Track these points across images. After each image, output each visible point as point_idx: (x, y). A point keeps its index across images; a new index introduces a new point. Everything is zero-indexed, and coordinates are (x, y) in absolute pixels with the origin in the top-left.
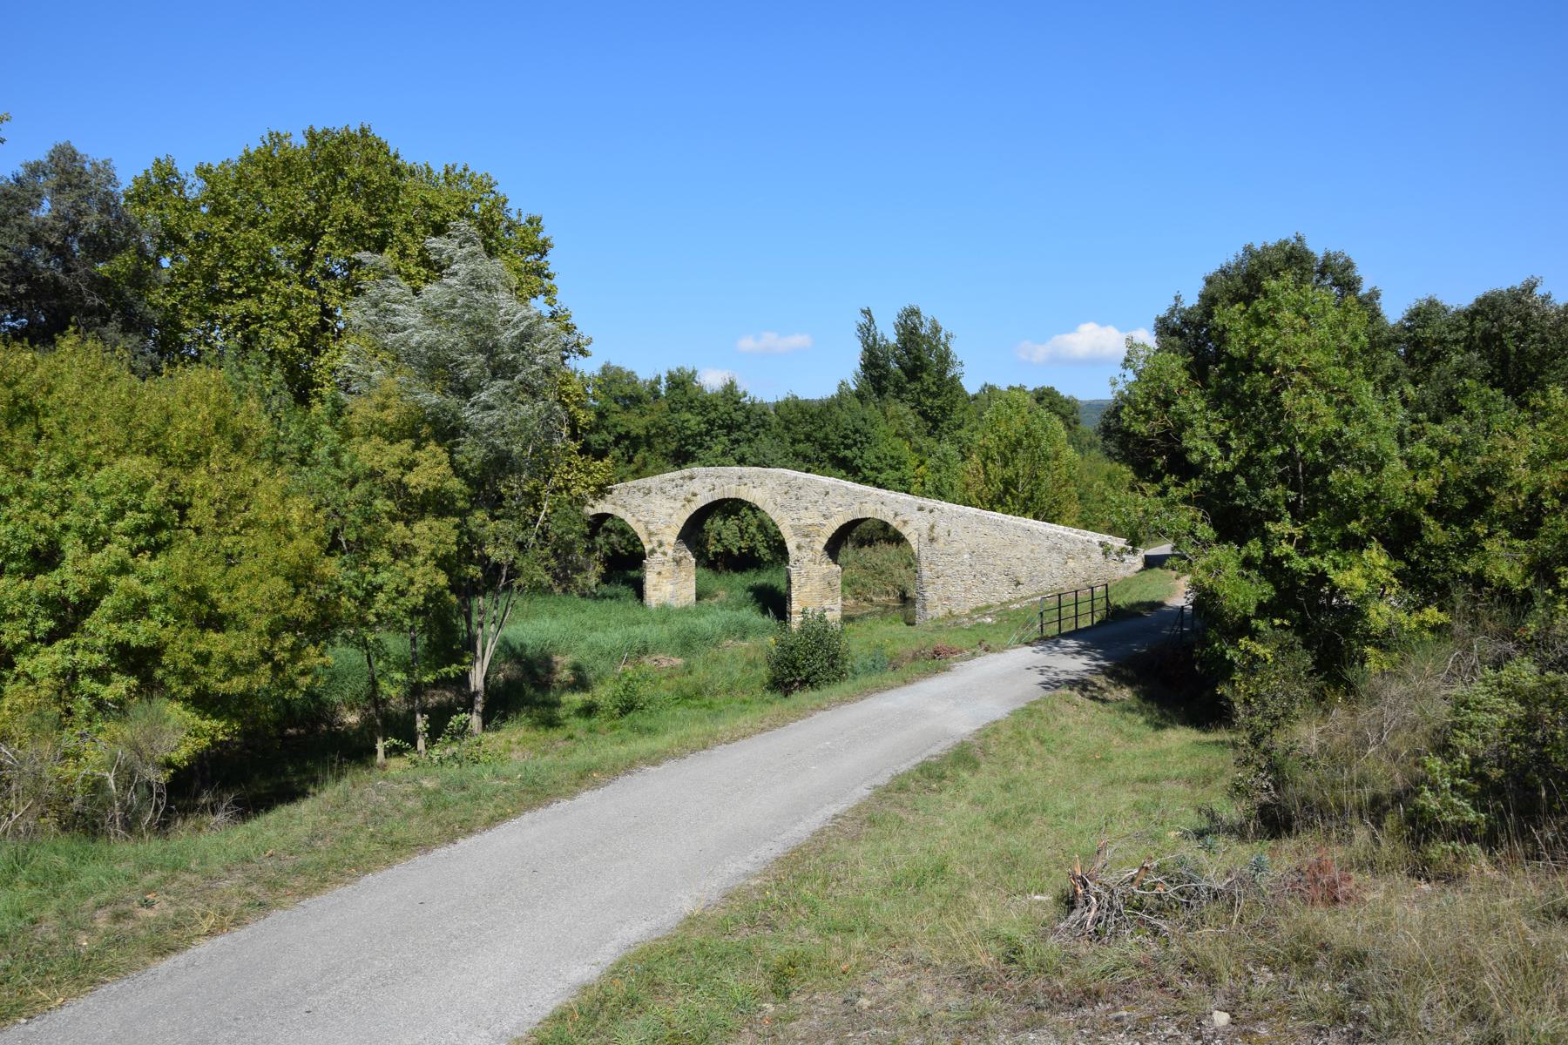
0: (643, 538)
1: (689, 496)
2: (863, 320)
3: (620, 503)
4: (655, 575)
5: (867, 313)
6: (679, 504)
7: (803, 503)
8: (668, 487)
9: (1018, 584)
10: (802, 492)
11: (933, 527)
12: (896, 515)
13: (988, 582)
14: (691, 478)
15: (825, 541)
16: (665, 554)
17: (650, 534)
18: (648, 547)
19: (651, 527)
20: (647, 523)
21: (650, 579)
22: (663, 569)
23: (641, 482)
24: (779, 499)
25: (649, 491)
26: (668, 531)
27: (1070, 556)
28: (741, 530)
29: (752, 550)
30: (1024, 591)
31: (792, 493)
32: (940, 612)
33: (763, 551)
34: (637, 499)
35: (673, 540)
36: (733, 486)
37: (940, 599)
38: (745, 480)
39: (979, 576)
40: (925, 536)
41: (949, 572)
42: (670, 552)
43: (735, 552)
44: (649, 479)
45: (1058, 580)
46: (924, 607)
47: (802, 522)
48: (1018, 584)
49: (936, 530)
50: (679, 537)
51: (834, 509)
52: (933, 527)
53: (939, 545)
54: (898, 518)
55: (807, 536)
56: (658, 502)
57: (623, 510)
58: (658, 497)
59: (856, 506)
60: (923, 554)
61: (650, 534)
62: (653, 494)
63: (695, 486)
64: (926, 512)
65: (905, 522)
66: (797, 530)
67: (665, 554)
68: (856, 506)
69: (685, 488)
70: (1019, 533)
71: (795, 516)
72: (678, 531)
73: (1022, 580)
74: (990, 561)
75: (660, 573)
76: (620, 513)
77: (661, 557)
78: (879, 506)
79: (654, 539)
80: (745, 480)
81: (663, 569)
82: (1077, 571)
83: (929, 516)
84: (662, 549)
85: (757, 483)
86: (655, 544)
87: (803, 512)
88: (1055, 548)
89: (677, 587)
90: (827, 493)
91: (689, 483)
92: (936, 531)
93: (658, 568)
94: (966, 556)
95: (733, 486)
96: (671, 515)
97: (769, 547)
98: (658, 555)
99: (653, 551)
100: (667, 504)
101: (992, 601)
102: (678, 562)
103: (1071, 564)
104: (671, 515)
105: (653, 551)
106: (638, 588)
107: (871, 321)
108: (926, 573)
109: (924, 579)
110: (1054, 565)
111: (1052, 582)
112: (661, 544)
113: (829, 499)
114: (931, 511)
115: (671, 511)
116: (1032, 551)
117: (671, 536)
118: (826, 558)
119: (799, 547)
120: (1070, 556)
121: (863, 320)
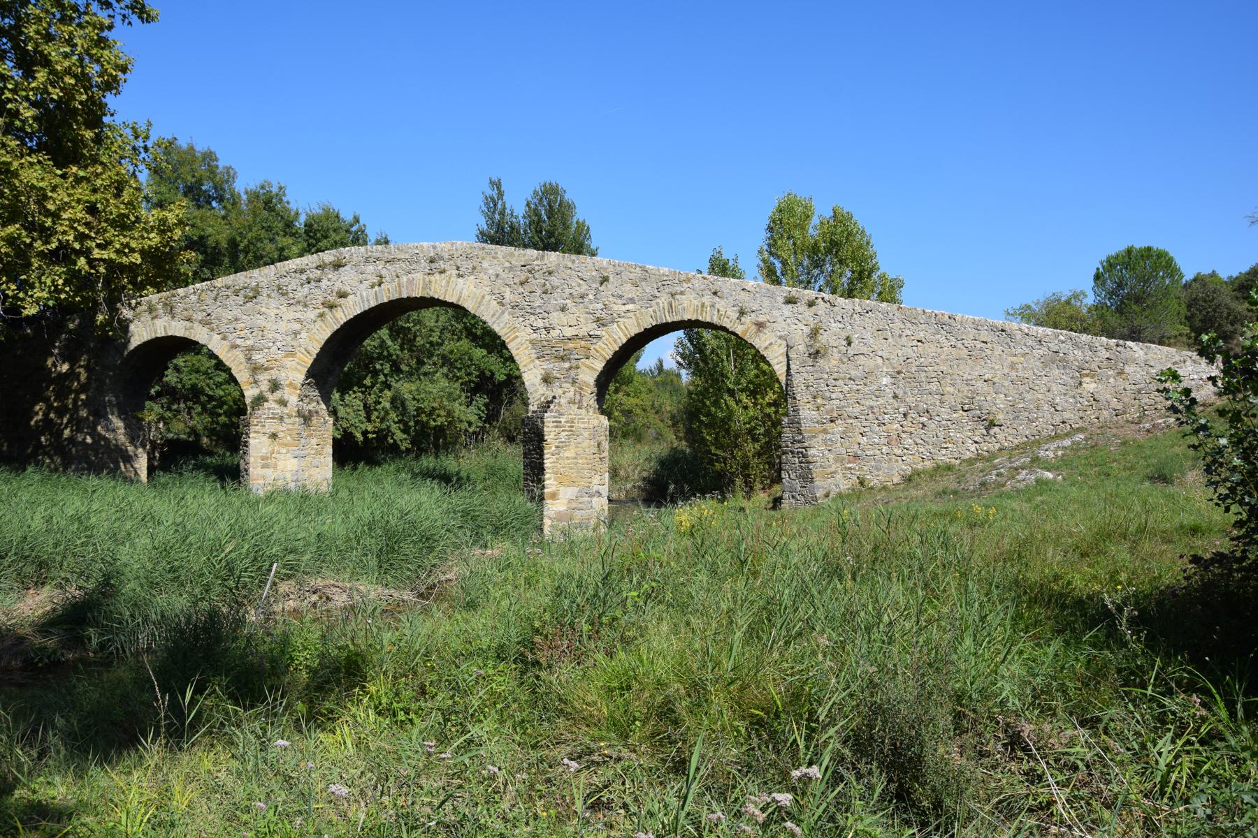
0: (242, 375)
1: (332, 298)
2: (489, 192)
3: (201, 315)
4: (265, 439)
5: (496, 185)
6: (312, 314)
7: (556, 300)
8: (293, 283)
9: (992, 424)
10: (555, 280)
11: (814, 333)
12: (742, 313)
13: (932, 425)
14: (337, 266)
15: (600, 366)
16: (283, 403)
17: (256, 369)
18: (250, 393)
19: (258, 357)
20: (250, 349)
21: (257, 443)
22: (281, 429)
23: (240, 278)
24: (508, 295)
25: (256, 293)
26: (289, 362)
27: (1082, 372)
28: (365, 406)
29: (383, 435)
30: (1003, 438)
31: (536, 283)
32: (844, 483)
33: (399, 436)
34: (231, 310)
35: (300, 377)
36: (419, 276)
37: (838, 459)
38: (442, 265)
39: (912, 414)
40: (802, 348)
41: (856, 410)
42: (293, 399)
43: (359, 437)
44: (256, 272)
45: (1066, 415)
46: (807, 478)
47: (554, 333)
48: (992, 424)
49: (823, 338)
50: (311, 373)
51: (618, 308)
52: (814, 333)
53: (830, 363)
54: (747, 319)
55: (562, 359)
56: (272, 312)
57: (205, 330)
58: (273, 303)
59: (664, 300)
60: (798, 380)
61: (256, 369)
62: (263, 299)
63: (346, 279)
64: (802, 307)
65: (760, 326)
66: (542, 350)
67: (283, 403)
68: (664, 300)
69: (324, 283)
70: (985, 335)
71: (540, 324)
72: (309, 361)
73: (1000, 417)
74: (934, 387)
75: (274, 436)
76: (199, 334)
77: (278, 409)
78: (707, 299)
79: (264, 378)
80: (442, 265)
81: (281, 429)
82: (1106, 395)
83: (809, 313)
84: (278, 394)
85: (466, 266)
86: (265, 386)
87: (556, 317)
88: (1057, 359)
89: (304, 463)
90: (605, 280)
91: (331, 274)
92: (820, 337)
93: (271, 427)
95: (419, 276)
96: (296, 333)
97: (406, 430)
98: (271, 405)
99: (260, 400)
100: (289, 314)
101: (943, 457)
102: (306, 418)
103: (1090, 386)
104: (296, 333)
105: (260, 400)
106: (232, 474)
107: (501, 194)
108: (807, 413)
109: (805, 425)
111: (1058, 419)
112: (275, 386)
115: (297, 326)
116: (1013, 366)
117: (295, 371)
118: (590, 400)
119: (547, 380)
120: (1082, 372)
121: (490, 192)
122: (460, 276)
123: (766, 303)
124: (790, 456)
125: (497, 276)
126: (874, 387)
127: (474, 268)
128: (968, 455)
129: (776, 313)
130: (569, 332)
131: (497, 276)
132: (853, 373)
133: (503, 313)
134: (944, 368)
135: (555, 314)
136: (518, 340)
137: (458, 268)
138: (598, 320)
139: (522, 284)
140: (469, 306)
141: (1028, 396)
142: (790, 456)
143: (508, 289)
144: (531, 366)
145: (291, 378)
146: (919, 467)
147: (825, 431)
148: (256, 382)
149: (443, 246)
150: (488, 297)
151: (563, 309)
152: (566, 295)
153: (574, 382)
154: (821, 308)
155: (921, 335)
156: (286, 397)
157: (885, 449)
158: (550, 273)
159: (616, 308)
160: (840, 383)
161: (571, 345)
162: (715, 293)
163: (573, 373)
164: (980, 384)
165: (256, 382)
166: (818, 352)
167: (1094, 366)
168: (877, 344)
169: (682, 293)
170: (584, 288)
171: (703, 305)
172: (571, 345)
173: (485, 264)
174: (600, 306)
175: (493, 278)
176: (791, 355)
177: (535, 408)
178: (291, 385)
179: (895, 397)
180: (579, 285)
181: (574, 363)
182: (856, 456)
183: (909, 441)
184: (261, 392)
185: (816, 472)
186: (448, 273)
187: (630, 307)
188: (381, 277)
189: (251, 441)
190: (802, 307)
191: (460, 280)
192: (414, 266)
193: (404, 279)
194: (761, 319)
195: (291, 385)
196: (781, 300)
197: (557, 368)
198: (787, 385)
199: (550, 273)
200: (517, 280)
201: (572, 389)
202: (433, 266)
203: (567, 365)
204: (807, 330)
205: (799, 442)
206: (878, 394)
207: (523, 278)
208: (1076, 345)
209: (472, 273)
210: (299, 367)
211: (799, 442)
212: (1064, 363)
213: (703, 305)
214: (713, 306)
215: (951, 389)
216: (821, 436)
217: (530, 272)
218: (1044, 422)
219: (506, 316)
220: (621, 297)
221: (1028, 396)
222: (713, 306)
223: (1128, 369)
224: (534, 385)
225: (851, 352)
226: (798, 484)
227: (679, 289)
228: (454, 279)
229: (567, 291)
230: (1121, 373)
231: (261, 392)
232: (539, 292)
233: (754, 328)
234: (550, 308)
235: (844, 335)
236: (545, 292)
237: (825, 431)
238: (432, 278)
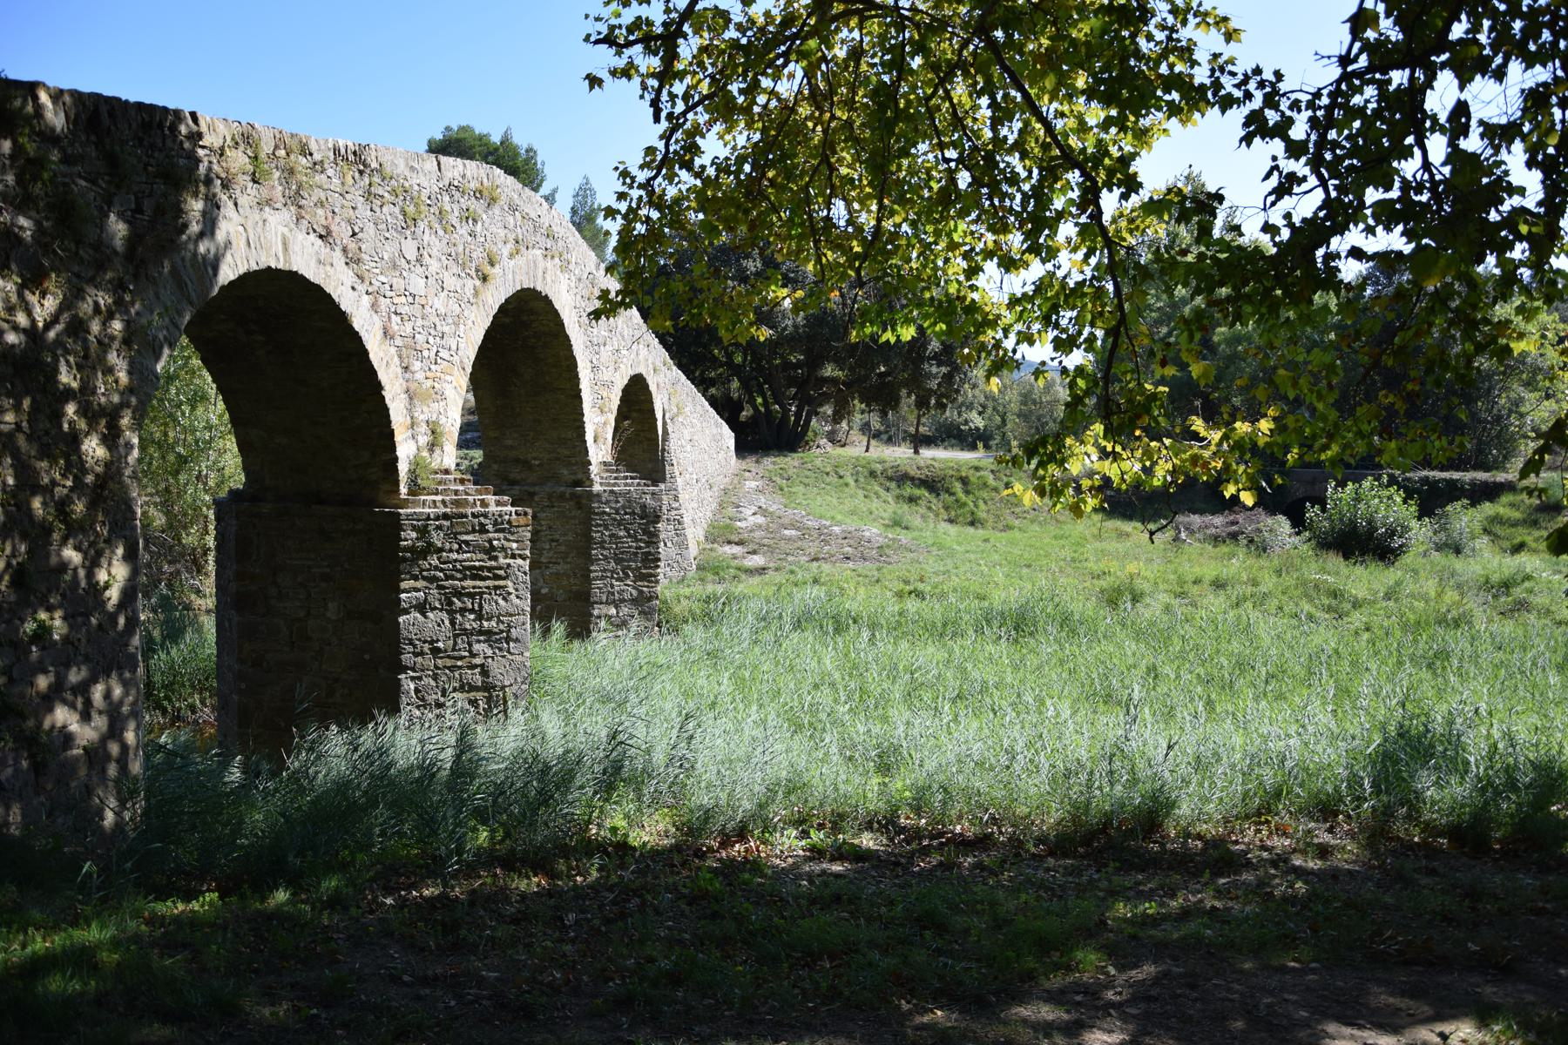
17: (411, 396)
205: (677, 509)
211: (677, 509)
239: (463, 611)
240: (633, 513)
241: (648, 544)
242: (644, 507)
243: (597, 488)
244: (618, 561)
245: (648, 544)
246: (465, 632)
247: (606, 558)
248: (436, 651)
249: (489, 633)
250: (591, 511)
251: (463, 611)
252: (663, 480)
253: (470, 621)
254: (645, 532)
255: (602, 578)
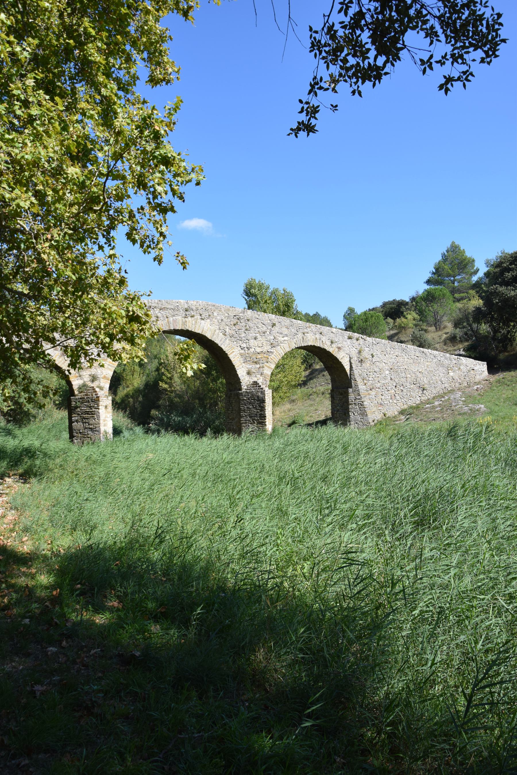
11: (360, 352)
12: (332, 342)
24: (227, 330)
30: (428, 395)
32: (378, 416)
36: (179, 318)
40: (356, 358)
41: (378, 385)
45: (446, 385)
46: (364, 414)
47: (252, 350)
52: (360, 352)
53: (367, 365)
54: (333, 345)
59: (300, 335)
60: (356, 372)
65: (339, 348)
68: (300, 335)
71: (244, 345)
74: (403, 375)
78: (318, 336)
82: (456, 377)
83: (357, 343)
85: (205, 314)
87: (252, 342)
88: (440, 364)
90: (274, 325)
94: (387, 372)
101: (411, 403)
103: (451, 374)
108: (361, 387)
110: (441, 374)
113: (276, 329)
114: (357, 340)
119: (249, 373)
120: (448, 369)
122: (202, 319)
123: (341, 339)
124: (353, 406)
125: (222, 320)
126: (383, 375)
127: (209, 316)
128: (418, 402)
129: (344, 343)
130: (259, 350)
131: (222, 320)
132: (377, 369)
133: (226, 339)
134: (406, 367)
135: (252, 341)
136: (234, 353)
137: (201, 315)
138: (272, 344)
139: (234, 325)
140: (209, 335)
141: (434, 378)
142: (353, 406)
143: (228, 327)
144: (241, 366)
145: (104, 374)
146: (402, 407)
147: (369, 394)
148: (80, 376)
149: (193, 303)
150: (217, 331)
151: (255, 338)
152: (257, 332)
153: (262, 374)
154: (361, 341)
155: (397, 354)
156: (102, 385)
157: (391, 401)
158: (248, 320)
159: (279, 339)
160: (371, 374)
161: (259, 356)
162: (321, 333)
163: (261, 369)
164: (418, 374)
165: (80, 376)
166: (362, 360)
167: (451, 366)
168: (382, 357)
169: (307, 333)
170: (264, 329)
171: (316, 339)
172: (259, 356)
173: (215, 314)
174: (272, 337)
175: (220, 321)
176: (352, 362)
177: (246, 387)
178: (105, 377)
179: (391, 379)
180: (262, 327)
181: (261, 365)
182: (381, 404)
183: (398, 397)
184: (84, 382)
185: (368, 411)
186: (196, 317)
187: (286, 338)
188: (157, 317)
189: (100, 411)
190: (355, 341)
191: (202, 321)
192: (176, 313)
193: (171, 319)
194: (340, 345)
195: (105, 377)
196: (346, 337)
197: (254, 367)
198: (351, 374)
199: (248, 320)
200: (232, 323)
201: (261, 378)
202: (187, 313)
203: (258, 366)
204: (357, 351)
206: (385, 378)
207: (235, 322)
208: (446, 358)
209: (208, 318)
210: (110, 367)
212: (442, 365)
213: (316, 339)
214: (320, 339)
215: (409, 376)
216: (368, 397)
217: (238, 319)
218: (439, 389)
219: (227, 341)
220: (281, 333)
221: (434, 378)
222: (320, 339)
223: (462, 367)
224: (243, 376)
225: (374, 360)
226: (359, 418)
227: (306, 330)
228: (199, 320)
229: (257, 329)
230: (460, 369)
231: (84, 382)
232: (244, 329)
233: (337, 349)
234: (249, 338)
235: (371, 353)
236: (246, 330)
237: (369, 394)
238: (186, 319)
239: (85, 423)
240: (254, 399)
241: (261, 410)
242: (258, 397)
243: (244, 390)
244: (251, 417)
245: (261, 410)
246: (86, 428)
247: (246, 416)
248: (80, 433)
249: (91, 429)
250: (239, 398)
251: (85, 423)
252: (351, 387)
253: (87, 425)
254: (260, 406)
255: (245, 423)
